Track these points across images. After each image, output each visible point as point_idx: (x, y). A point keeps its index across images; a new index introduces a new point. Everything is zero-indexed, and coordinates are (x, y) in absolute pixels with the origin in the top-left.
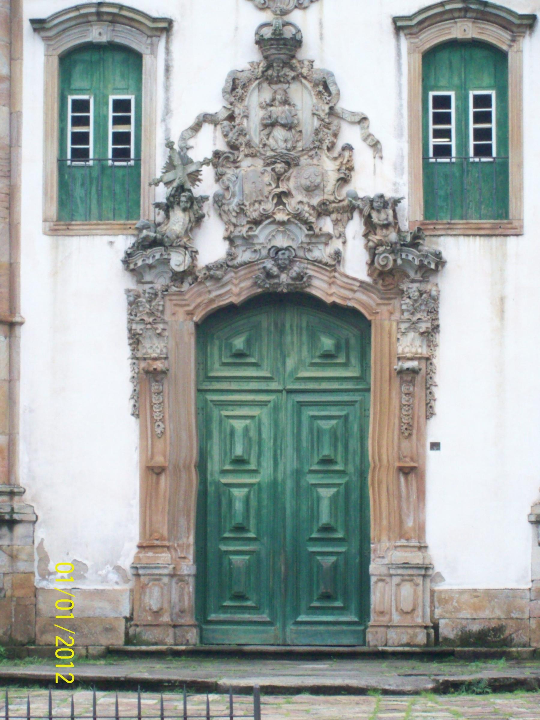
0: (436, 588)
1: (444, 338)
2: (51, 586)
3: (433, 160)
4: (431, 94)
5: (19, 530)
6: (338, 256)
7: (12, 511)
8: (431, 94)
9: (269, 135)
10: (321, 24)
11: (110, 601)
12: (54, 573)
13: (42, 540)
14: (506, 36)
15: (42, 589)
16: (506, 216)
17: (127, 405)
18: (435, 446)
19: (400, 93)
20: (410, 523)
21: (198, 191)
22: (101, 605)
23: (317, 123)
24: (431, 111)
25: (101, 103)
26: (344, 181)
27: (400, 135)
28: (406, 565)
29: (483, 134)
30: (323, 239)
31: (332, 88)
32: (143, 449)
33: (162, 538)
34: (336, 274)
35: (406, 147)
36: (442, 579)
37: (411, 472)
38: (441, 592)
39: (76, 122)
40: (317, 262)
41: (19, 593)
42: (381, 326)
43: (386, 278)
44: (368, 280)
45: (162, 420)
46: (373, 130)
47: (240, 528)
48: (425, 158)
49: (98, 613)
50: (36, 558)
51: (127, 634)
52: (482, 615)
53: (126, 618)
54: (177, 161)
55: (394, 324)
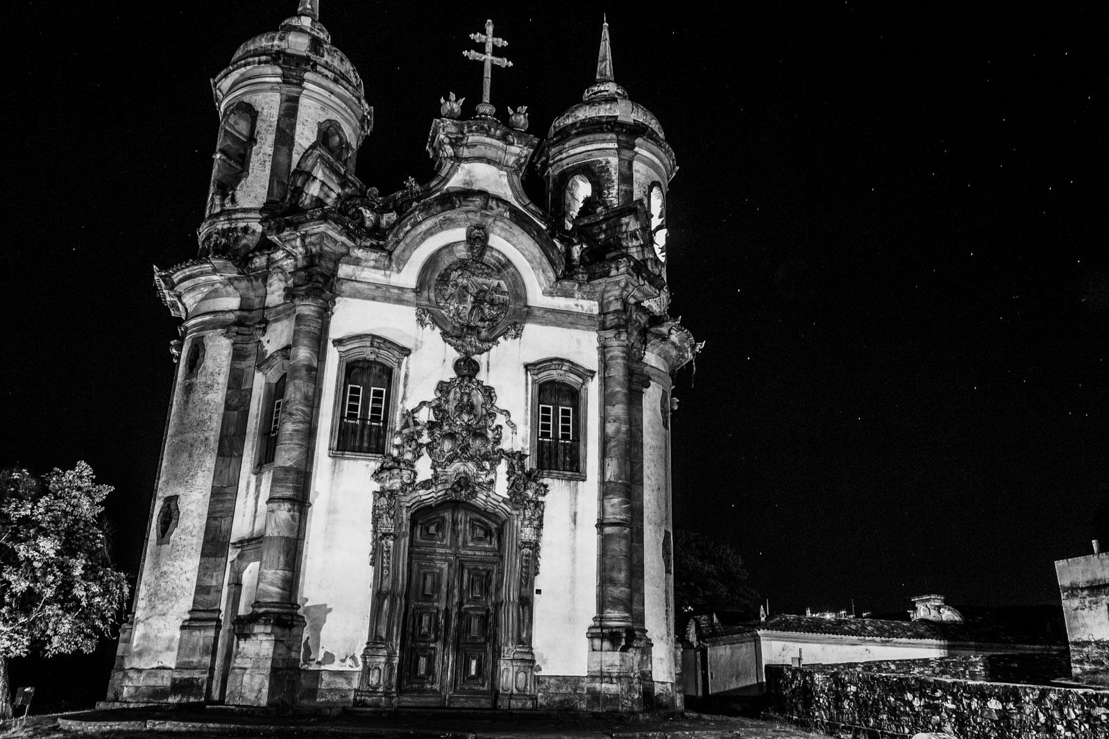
0: (536, 674)
1: (545, 531)
2: (311, 668)
3: (540, 439)
4: (541, 406)
5: (295, 631)
6: (492, 482)
7: (292, 620)
8: (541, 406)
9: (459, 416)
10: (488, 363)
11: (346, 678)
12: (314, 660)
13: (308, 638)
14: (581, 381)
15: (304, 670)
16: (578, 471)
17: (368, 558)
18: (539, 592)
19: (527, 404)
20: (524, 636)
21: (420, 441)
22: (341, 680)
23: (484, 412)
24: (541, 414)
25: (367, 391)
26: (497, 441)
27: (526, 424)
28: (522, 660)
29: (565, 429)
30: (485, 472)
31: (493, 394)
32: (375, 585)
33: (381, 638)
34: (490, 493)
35: (529, 430)
36: (540, 669)
37: (526, 603)
38: (539, 677)
39: (352, 399)
40: (479, 484)
41: (291, 673)
42: (513, 523)
43: (516, 497)
44: (508, 497)
45: (388, 569)
46: (513, 419)
47: (425, 636)
48: (538, 437)
49: (339, 686)
50: (302, 650)
51: (355, 699)
52: (561, 691)
53: (355, 689)
54: (411, 423)
55: (520, 523)
